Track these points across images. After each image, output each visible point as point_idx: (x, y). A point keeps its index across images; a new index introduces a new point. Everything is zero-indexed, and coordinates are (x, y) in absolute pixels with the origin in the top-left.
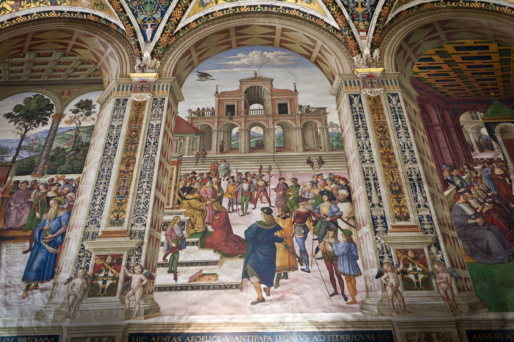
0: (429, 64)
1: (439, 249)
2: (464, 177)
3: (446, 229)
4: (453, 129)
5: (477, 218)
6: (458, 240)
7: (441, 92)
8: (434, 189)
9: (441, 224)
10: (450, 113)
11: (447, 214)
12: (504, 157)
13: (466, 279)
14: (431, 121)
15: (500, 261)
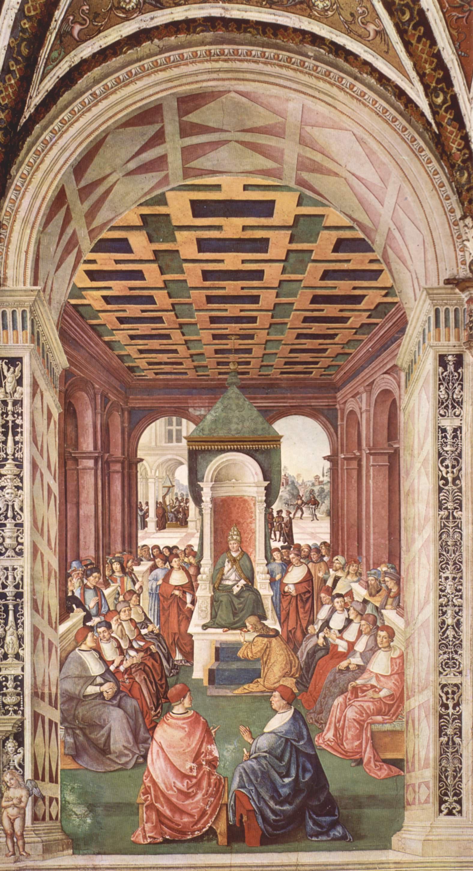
0: (117, 262)
1: (21, 744)
2: (107, 592)
3: (42, 703)
4: (118, 467)
5: (106, 681)
6: (59, 726)
7: (120, 357)
8: (43, 618)
9: (37, 695)
10: (123, 422)
11: (54, 673)
12: (201, 545)
13: (51, 800)
14: (76, 445)
15: (120, 767)
